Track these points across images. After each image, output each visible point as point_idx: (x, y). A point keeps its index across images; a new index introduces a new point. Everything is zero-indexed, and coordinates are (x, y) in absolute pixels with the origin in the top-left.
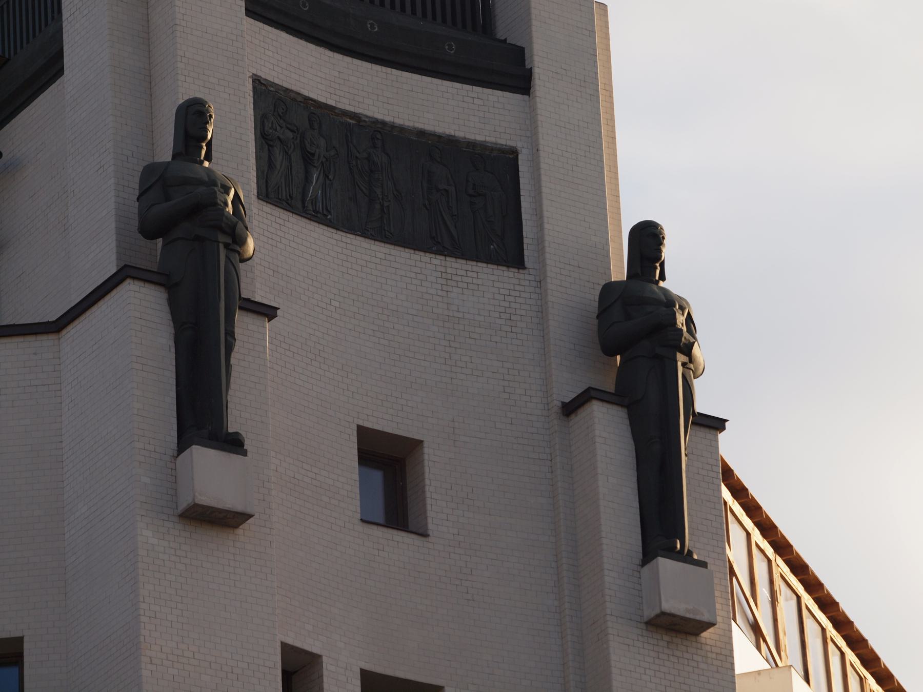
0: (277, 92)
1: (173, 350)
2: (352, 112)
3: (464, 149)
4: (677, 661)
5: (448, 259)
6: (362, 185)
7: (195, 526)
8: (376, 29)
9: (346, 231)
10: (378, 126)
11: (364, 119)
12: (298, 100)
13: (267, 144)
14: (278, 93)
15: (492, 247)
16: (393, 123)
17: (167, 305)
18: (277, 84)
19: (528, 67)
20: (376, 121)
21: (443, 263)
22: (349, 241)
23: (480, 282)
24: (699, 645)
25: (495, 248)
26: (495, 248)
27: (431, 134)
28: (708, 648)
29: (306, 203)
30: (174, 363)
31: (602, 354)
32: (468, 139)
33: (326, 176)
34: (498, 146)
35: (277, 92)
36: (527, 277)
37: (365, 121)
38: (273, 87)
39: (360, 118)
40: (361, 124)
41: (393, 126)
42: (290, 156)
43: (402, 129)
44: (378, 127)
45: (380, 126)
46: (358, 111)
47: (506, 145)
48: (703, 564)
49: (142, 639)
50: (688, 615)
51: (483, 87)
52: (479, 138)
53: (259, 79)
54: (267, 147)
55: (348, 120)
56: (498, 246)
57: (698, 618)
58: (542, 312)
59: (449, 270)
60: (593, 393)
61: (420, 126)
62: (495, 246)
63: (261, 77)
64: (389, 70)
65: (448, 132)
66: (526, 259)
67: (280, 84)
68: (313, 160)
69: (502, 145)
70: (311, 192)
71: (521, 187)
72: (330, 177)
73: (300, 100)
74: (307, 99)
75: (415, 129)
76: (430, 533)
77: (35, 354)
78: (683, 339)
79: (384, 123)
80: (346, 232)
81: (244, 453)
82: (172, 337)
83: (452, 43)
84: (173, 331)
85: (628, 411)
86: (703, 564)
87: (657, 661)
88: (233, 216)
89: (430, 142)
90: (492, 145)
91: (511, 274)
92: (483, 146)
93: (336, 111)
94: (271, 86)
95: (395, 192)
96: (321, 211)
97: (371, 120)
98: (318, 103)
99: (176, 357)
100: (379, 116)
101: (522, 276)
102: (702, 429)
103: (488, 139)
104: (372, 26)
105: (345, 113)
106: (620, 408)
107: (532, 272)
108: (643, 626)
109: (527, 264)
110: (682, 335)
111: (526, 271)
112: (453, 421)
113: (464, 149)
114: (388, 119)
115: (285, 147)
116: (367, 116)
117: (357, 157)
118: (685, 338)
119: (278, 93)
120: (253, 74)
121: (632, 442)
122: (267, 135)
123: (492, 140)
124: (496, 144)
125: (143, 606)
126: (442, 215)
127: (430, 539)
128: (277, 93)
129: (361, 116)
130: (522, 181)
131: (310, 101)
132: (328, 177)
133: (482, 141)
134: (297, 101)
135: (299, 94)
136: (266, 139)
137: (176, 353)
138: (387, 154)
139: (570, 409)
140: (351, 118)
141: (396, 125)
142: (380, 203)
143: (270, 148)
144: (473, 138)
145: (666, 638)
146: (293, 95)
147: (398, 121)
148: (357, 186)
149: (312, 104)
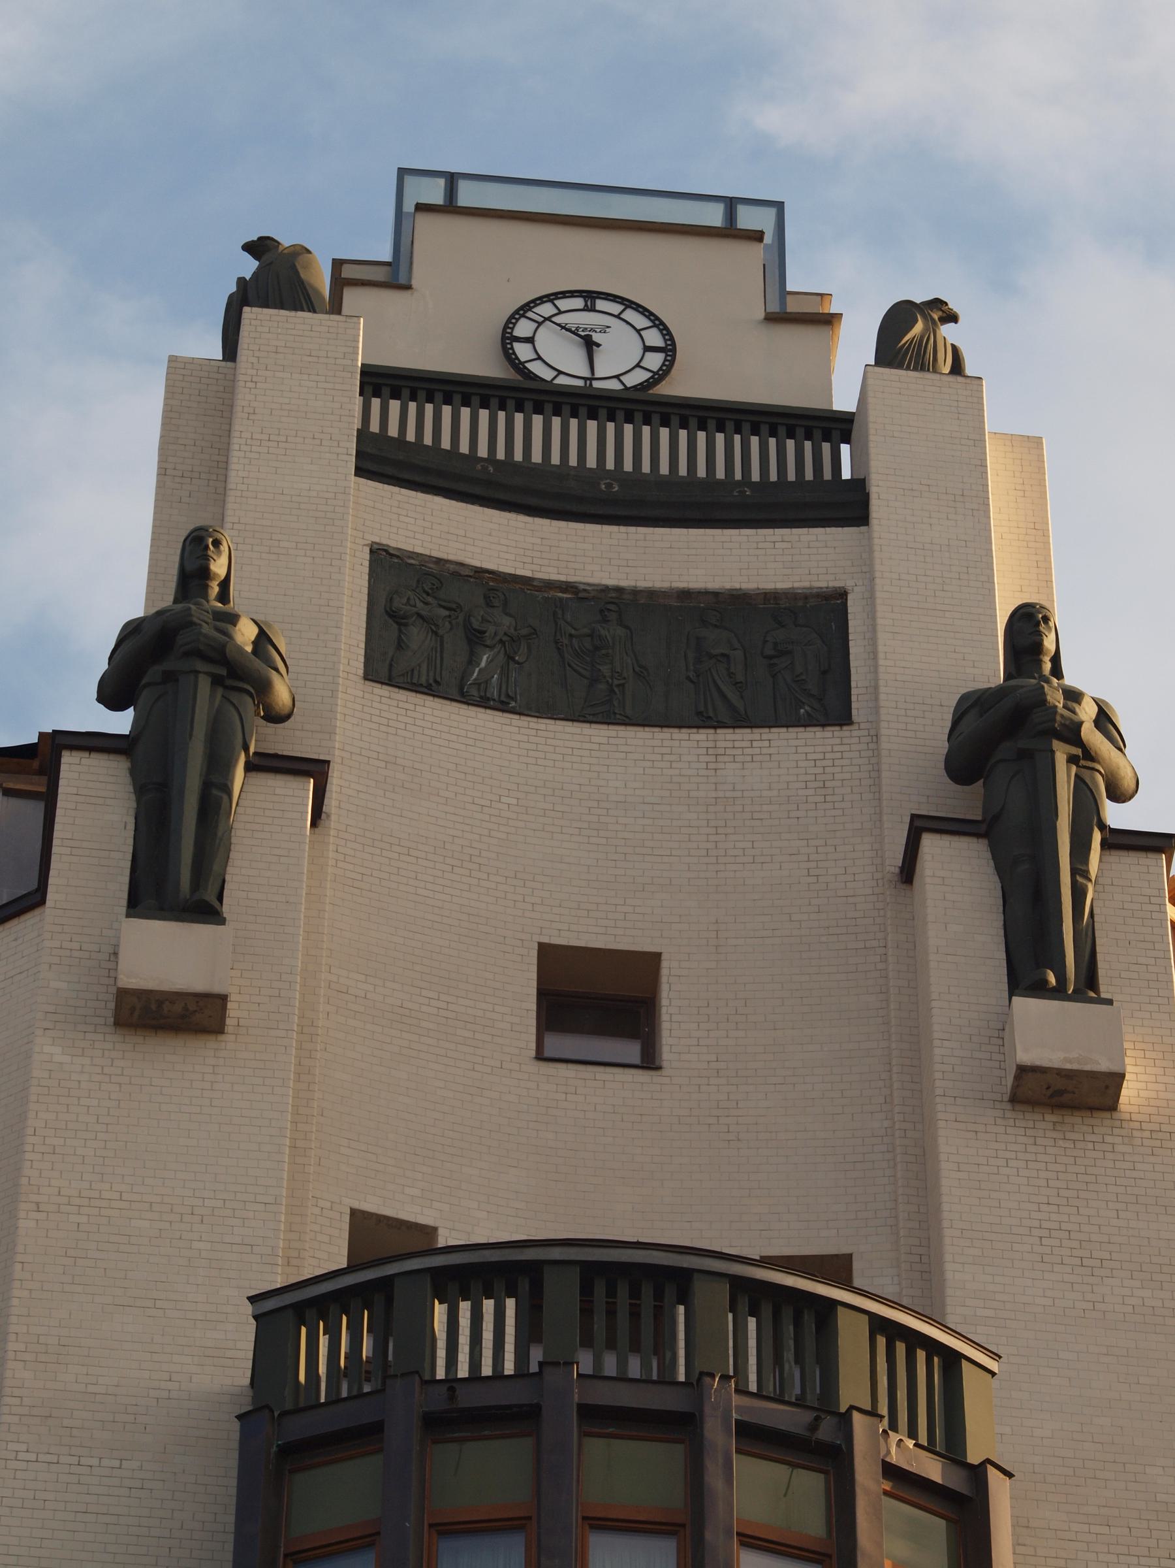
0: (423, 565)
1: (131, 826)
2: (563, 582)
3: (761, 606)
4: (1072, 1146)
5: (719, 731)
6: (577, 665)
7: (145, 1036)
8: (616, 489)
9: (537, 714)
10: (610, 595)
11: (582, 587)
12: (462, 573)
13: (397, 623)
14: (426, 566)
15: (802, 711)
16: (636, 587)
17: (128, 775)
18: (421, 554)
19: (867, 491)
20: (606, 589)
21: (711, 737)
22: (543, 727)
23: (772, 751)
24: (1118, 1123)
25: (807, 712)
26: (807, 712)
27: (699, 592)
28: (1133, 1125)
29: (466, 687)
30: (131, 841)
31: (944, 772)
32: (763, 589)
33: (510, 658)
34: (815, 591)
35: (423, 565)
36: (855, 733)
37: (585, 590)
38: (413, 559)
39: (576, 588)
40: (581, 595)
41: (636, 592)
42: (442, 637)
43: (652, 593)
44: (611, 598)
45: (614, 595)
46: (571, 579)
47: (827, 588)
48: (1110, 1002)
49: (24, 1181)
50: (1068, 1066)
51: (791, 528)
52: (782, 585)
53: (385, 548)
54: (395, 626)
55: (560, 595)
56: (812, 707)
57: (1088, 1068)
58: (876, 771)
59: (719, 744)
60: (918, 823)
61: (682, 585)
62: (807, 708)
63: (388, 546)
64: (632, 529)
65: (728, 586)
66: (854, 712)
67: (428, 553)
68: (482, 638)
69: (821, 588)
70: (475, 674)
71: (851, 630)
72: (517, 658)
73: (467, 573)
74: (480, 572)
75: (673, 589)
76: (665, 1064)
77: (16, 940)
78: (1058, 718)
79: (619, 590)
80: (537, 717)
81: (222, 921)
82: (132, 812)
83: (746, 489)
84: (135, 805)
85: (989, 841)
86: (1110, 1002)
87: (1031, 1149)
88: (253, 657)
89: (702, 605)
90: (805, 591)
91: (829, 734)
92: (791, 596)
93: (535, 584)
94: (409, 557)
95: (637, 669)
96: (496, 696)
97: (596, 588)
98: (500, 576)
99: (134, 835)
100: (611, 582)
101: (847, 734)
102: (1132, 854)
103: (796, 585)
104: (609, 486)
105: (549, 585)
106: (974, 840)
107: (862, 725)
108: (1008, 1106)
109: (855, 717)
110: (1056, 712)
111: (855, 727)
112: (717, 922)
113: (761, 606)
114: (624, 583)
115: (433, 627)
116: (589, 584)
117: (571, 636)
118: (1062, 716)
119: (426, 566)
120: (372, 542)
121: (996, 879)
122: (396, 612)
123: (807, 584)
124: (811, 588)
125: (30, 1139)
126: (714, 681)
127: (664, 1072)
128: (423, 568)
129: (577, 585)
130: (851, 623)
131: (487, 575)
132: (513, 659)
133: (786, 589)
134: (460, 575)
135: (462, 564)
136: (395, 616)
137: (136, 830)
138: (627, 627)
139: (908, 872)
140: (564, 591)
141: (639, 589)
142: (607, 682)
143: (403, 628)
144: (773, 587)
145: (1048, 1117)
146: (452, 567)
147: (642, 584)
148: (568, 668)
149: (488, 577)
